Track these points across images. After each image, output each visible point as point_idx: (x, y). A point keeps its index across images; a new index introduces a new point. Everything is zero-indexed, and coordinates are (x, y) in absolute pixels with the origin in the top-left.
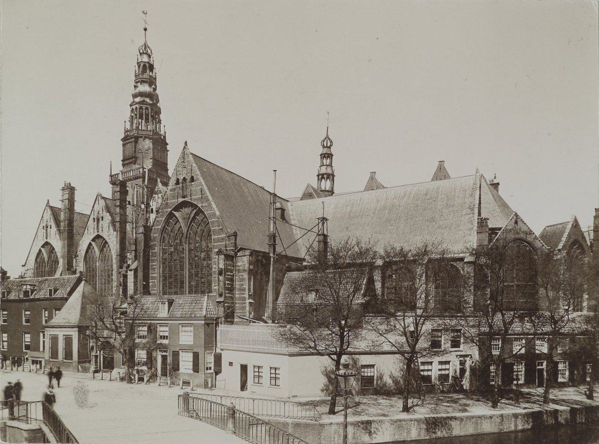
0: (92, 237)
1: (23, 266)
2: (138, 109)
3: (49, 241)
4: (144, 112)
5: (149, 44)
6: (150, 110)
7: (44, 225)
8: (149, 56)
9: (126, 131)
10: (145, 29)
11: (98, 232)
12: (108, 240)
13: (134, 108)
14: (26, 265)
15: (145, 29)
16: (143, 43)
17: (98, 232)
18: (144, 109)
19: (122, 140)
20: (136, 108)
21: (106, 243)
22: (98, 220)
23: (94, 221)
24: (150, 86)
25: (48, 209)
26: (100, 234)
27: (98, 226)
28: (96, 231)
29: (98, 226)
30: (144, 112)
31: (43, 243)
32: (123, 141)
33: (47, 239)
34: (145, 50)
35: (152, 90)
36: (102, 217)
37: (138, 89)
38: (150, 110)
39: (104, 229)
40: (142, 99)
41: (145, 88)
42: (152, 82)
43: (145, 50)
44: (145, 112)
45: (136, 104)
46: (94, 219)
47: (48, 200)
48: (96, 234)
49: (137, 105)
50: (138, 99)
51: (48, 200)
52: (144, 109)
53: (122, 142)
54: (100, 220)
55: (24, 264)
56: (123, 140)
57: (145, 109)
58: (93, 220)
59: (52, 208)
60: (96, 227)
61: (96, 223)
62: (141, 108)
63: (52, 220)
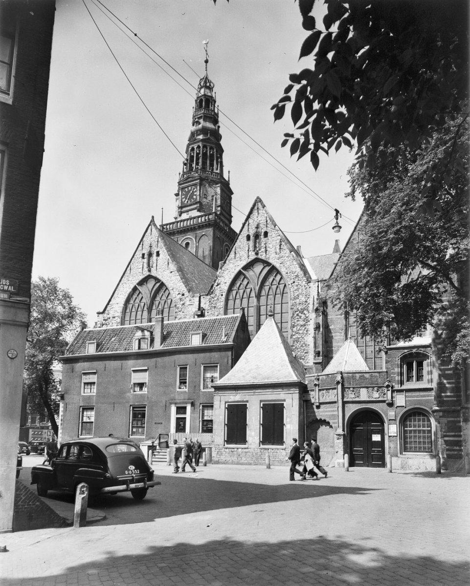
1: (99, 313)
2: (201, 147)
6: (215, 151)
7: (146, 252)
13: (195, 147)
14: (106, 312)
17: (257, 254)
18: (208, 149)
20: (199, 147)
31: (141, 277)
33: (150, 271)
35: (217, 127)
36: (266, 234)
39: (268, 249)
41: (209, 125)
42: (215, 119)
46: (248, 238)
47: (153, 217)
51: (153, 217)
52: (208, 149)
55: (101, 311)
61: (251, 243)
62: (204, 146)
63: (161, 244)
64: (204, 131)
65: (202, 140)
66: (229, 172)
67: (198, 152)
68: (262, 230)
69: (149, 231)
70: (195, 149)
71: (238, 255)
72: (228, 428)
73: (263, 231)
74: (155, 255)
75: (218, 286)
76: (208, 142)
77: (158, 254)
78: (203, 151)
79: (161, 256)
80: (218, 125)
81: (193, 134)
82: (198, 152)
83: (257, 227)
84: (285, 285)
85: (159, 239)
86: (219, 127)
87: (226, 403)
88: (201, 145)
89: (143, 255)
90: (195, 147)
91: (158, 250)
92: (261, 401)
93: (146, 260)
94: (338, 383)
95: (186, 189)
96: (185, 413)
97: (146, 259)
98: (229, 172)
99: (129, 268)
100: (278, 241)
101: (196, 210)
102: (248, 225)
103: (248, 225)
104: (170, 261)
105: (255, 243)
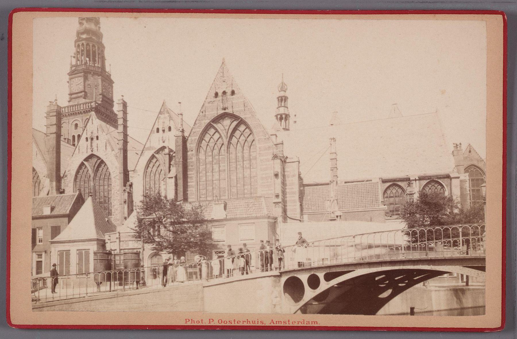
0: (86, 155)
4: (91, 49)
6: (96, 48)
9: (72, 66)
11: (92, 151)
12: (104, 160)
13: (80, 44)
17: (92, 151)
18: (91, 47)
19: (68, 74)
20: (83, 44)
21: (102, 162)
22: (92, 139)
24: (96, 25)
26: (95, 153)
27: (91, 146)
29: (91, 146)
30: (91, 49)
32: (69, 75)
35: (98, 28)
36: (97, 138)
37: (84, 26)
38: (96, 48)
39: (99, 148)
40: (88, 37)
44: (93, 49)
45: (82, 40)
46: (87, 139)
48: (90, 153)
49: (83, 42)
50: (84, 36)
52: (91, 47)
53: (68, 77)
54: (95, 139)
56: (70, 74)
57: (92, 47)
58: (85, 139)
60: (89, 147)
62: (88, 44)
64: (87, 31)
65: (85, 39)
68: (95, 136)
70: (80, 46)
71: (81, 151)
72: (60, 267)
73: (96, 135)
75: (69, 172)
76: (91, 41)
80: (98, 26)
81: (79, 33)
82: (82, 49)
83: (92, 133)
84: (110, 173)
86: (99, 27)
87: (58, 251)
88: (84, 43)
90: (80, 44)
92: (77, 250)
94: (117, 238)
96: (41, 258)
100: (105, 143)
104: (38, 152)
105: (91, 143)
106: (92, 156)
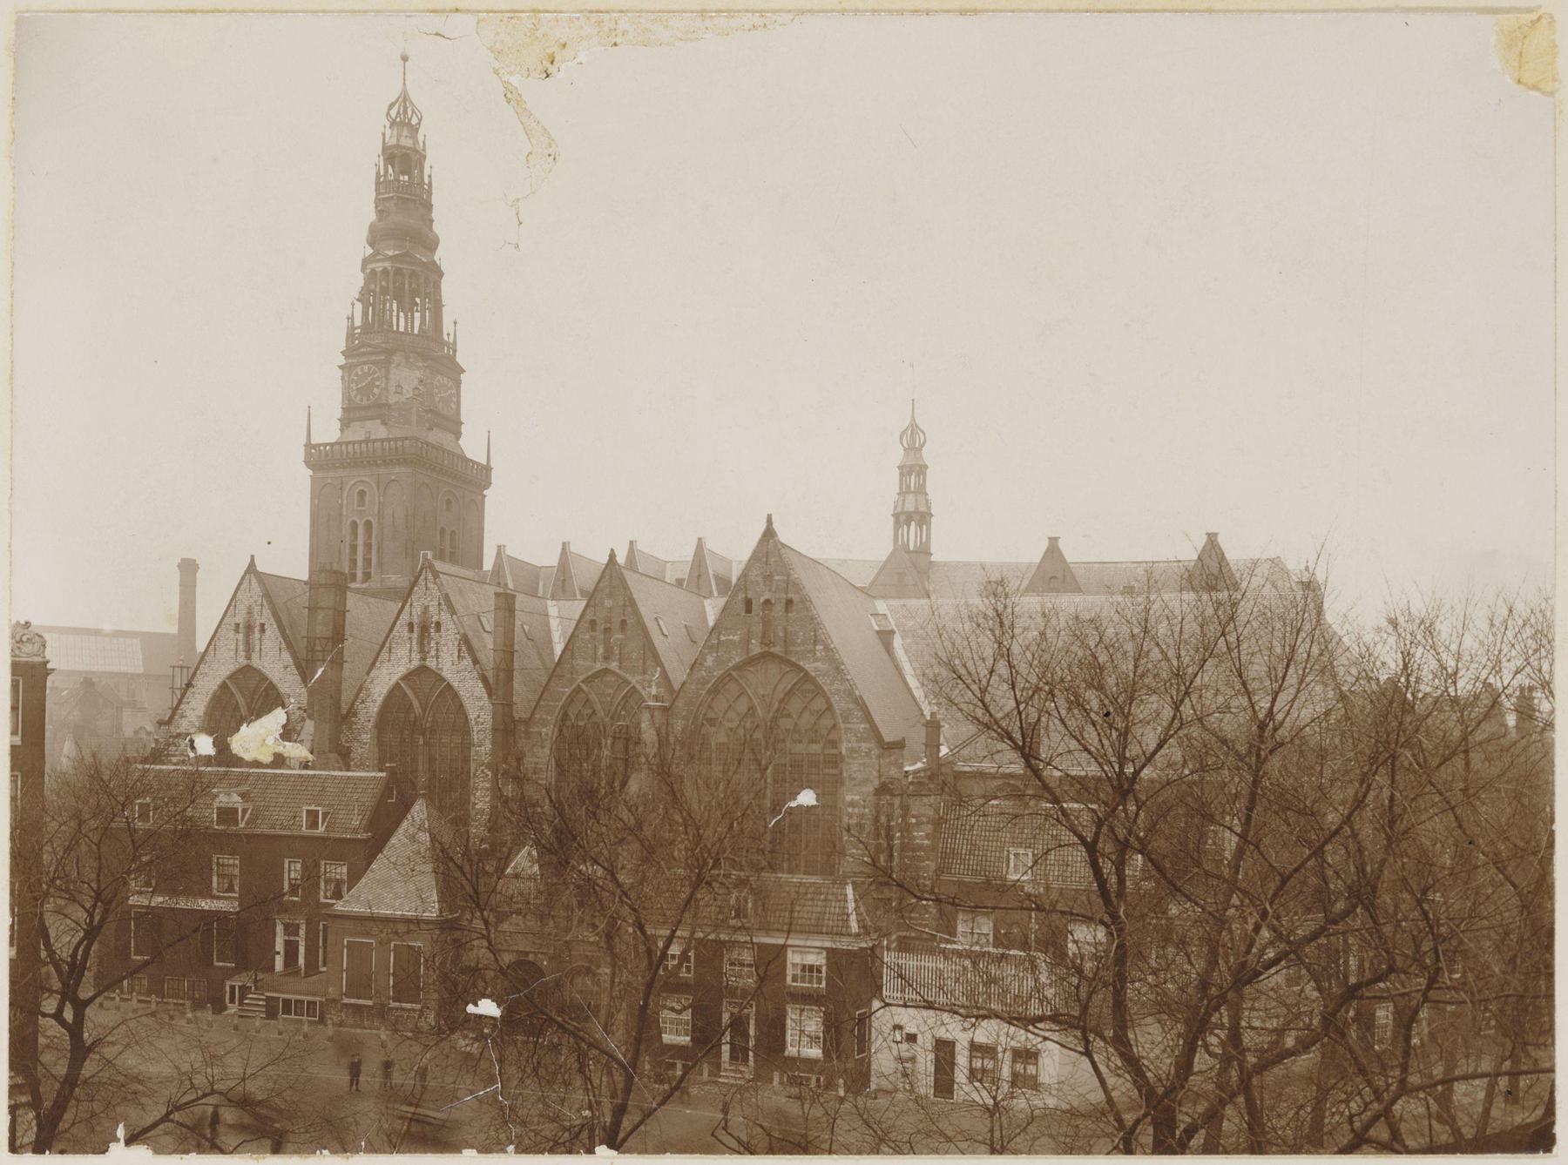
2: (391, 274)
3: (256, 662)
5: (413, 96)
7: (240, 618)
8: (414, 130)
10: (405, 59)
15: (405, 59)
16: (394, 94)
17: (424, 659)
23: (411, 629)
25: (254, 581)
28: (416, 656)
34: (404, 118)
36: (438, 625)
43: (404, 118)
46: (411, 626)
47: (252, 557)
51: (252, 557)
57: (410, 277)
58: (406, 628)
59: (261, 577)
62: (398, 271)
66: (455, 323)
67: (384, 283)
69: (246, 582)
74: (257, 629)
77: (263, 630)
78: (394, 283)
79: (268, 633)
85: (265, 603)
89: (237, 625)
91: (262, 621)
93: (241, 637)
95: (359, 370)
97: (241, 635)
98: (455, 323)
99: (212, 647)
101: (379, 421)
102: (411, 605)
103: (411, 605)
106: (423, 669)
